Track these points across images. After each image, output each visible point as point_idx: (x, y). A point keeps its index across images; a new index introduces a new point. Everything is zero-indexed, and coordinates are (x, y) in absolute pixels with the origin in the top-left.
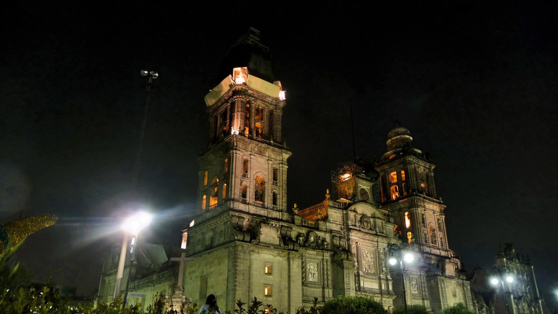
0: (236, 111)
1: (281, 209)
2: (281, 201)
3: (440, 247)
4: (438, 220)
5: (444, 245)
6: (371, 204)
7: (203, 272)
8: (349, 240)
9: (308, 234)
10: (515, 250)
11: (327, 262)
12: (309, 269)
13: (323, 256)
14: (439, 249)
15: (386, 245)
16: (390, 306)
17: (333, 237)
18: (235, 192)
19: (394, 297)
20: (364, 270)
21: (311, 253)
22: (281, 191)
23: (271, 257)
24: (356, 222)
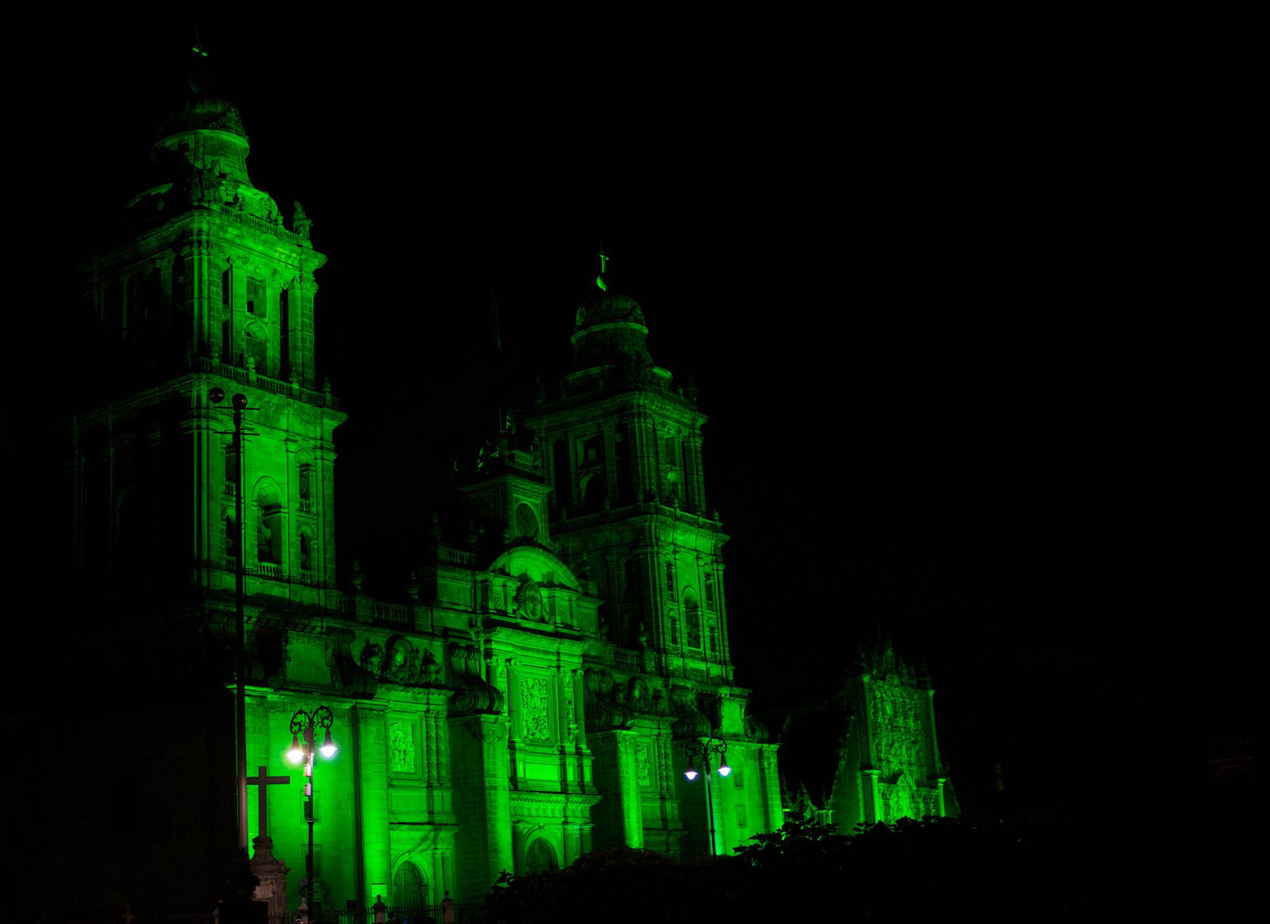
1: (322, 579)
2: (322, 555)
3: (708, 652)
4: (708, 576)
5: (720, 646)
6: (545, 549)
8: (489, 654)
9: (390, 645)
12: (395, 741)
14: (705, 660)
15: (578, 661)
17: (450, 649)
18: (211, 542)
20: (525, 733)
22: (321, 528)
24: (506, 604)
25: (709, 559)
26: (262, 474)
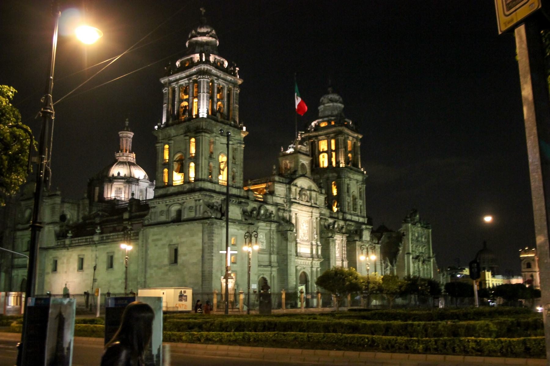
0: (202, 91)
3: (359, 214)
4: (360, 189)
6: (309, 178)
7: (172, 241)
8: (290, 211)
9: (260, 208)
10: (419, 216)
11: (273, 232)
13: (271, 227)
14: (358, 216)
15: (318, 215)
16: (318, 268)
17: (279, 209)
19: (322, 260)
21: (262, 225)
23: (236, 230)
24: (296, 195)
25: (360, 183)
26: (221, 151)
